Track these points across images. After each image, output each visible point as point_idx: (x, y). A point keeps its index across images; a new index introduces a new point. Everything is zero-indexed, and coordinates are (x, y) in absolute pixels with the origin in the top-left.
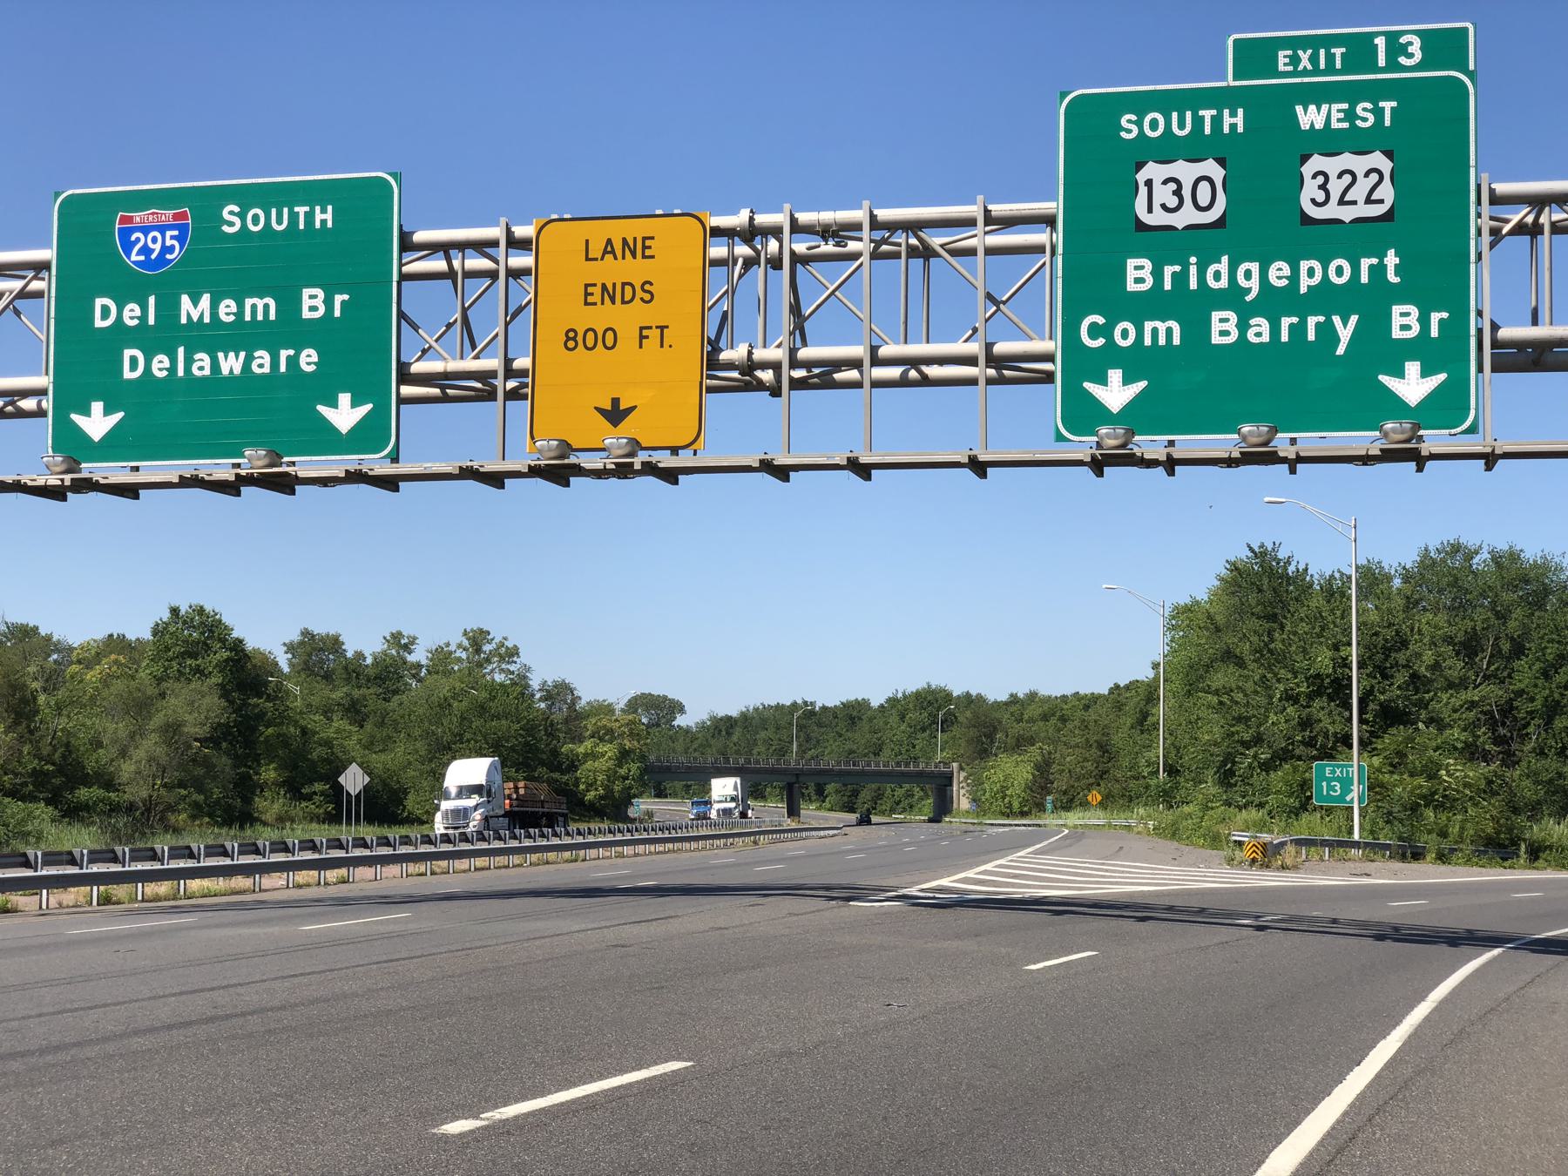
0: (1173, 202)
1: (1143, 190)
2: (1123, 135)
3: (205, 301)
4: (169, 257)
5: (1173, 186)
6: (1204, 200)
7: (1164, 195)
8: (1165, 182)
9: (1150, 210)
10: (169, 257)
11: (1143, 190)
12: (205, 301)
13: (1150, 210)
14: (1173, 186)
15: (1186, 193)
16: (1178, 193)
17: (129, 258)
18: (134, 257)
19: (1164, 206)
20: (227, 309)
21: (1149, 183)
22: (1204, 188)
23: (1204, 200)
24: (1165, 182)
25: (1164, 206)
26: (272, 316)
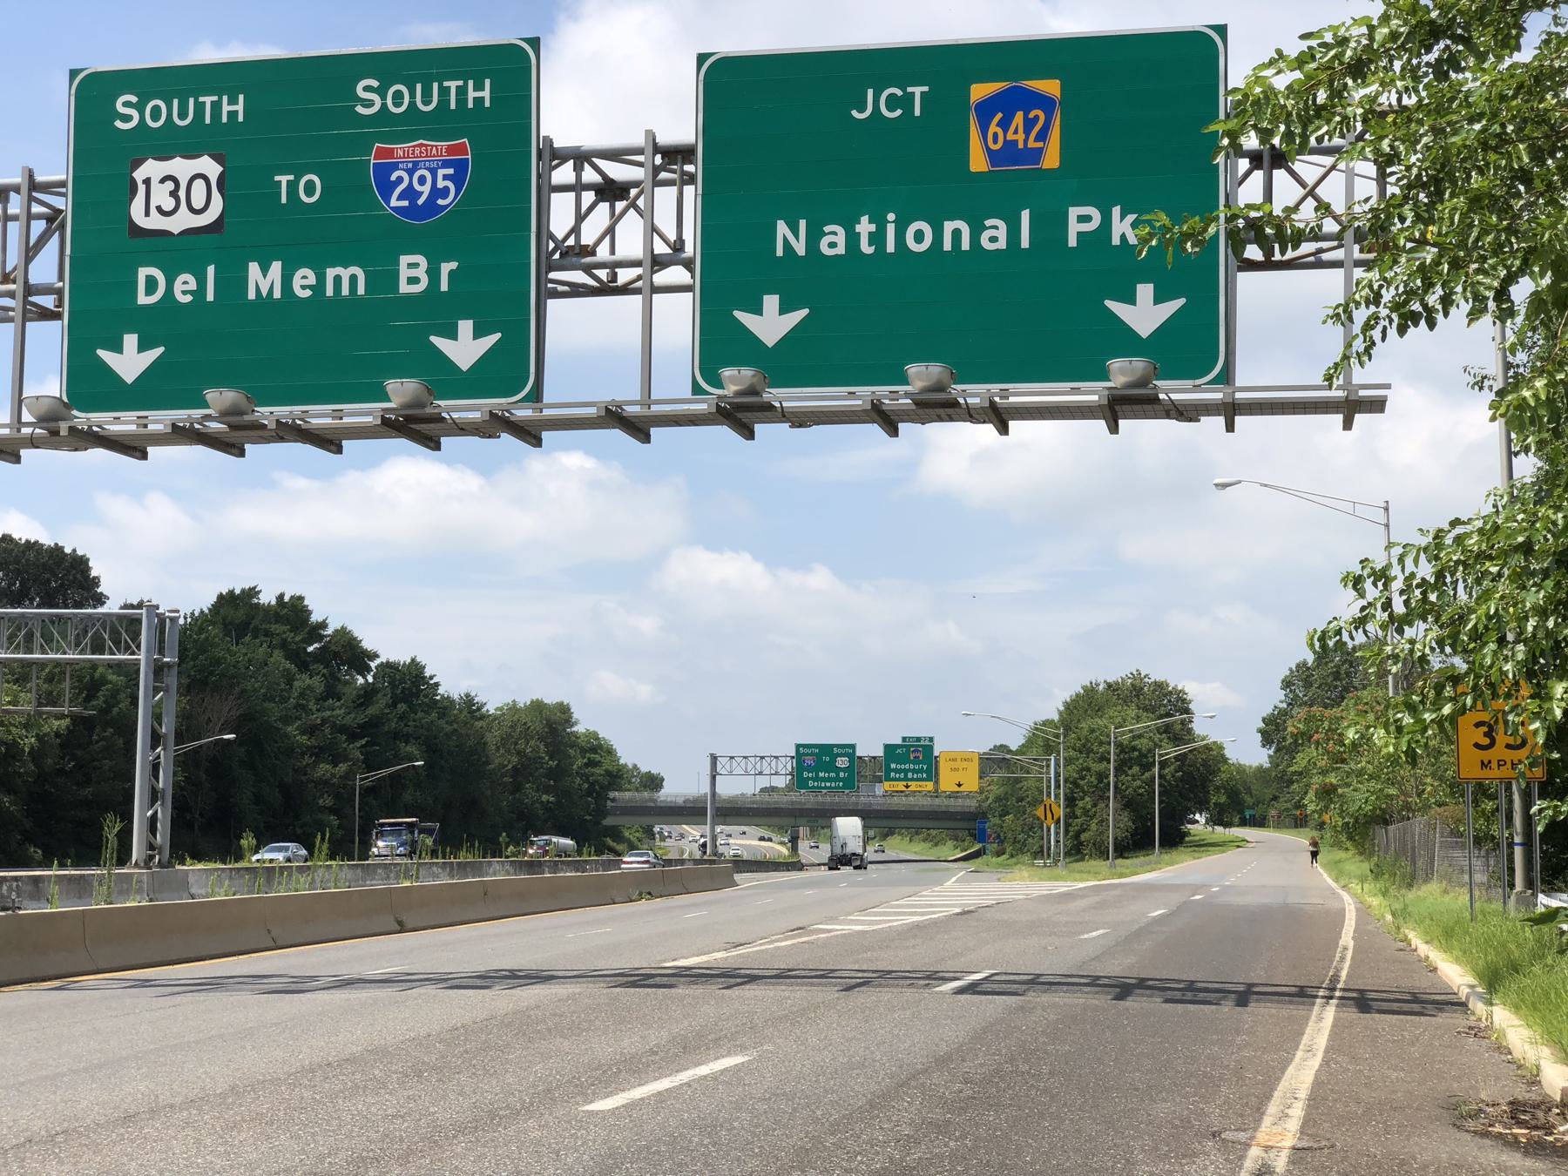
0: (169, 204)
1: (142, 188)
2: (119, 124)
3: (276, 268)
4: (440, 202)
5: (170, 185)
6: (198, 202)
7: (162, 197)
8: (163, 181)
9: (147, 214)
10: (440, 202)
11: (142, 188)
12: (276, 268)
13: (147, 214)
14: (170, 185)
15: (182, 194)
16: (174, 194)
17: (388, 203)
18: (394, 203)
19: (159, 209)
20: (303, 279)
21: (147, 182)
22: (199, 185)
23: (198, 202)
24: (163, 181)
25: (159, 209)
26: (361, 290)
